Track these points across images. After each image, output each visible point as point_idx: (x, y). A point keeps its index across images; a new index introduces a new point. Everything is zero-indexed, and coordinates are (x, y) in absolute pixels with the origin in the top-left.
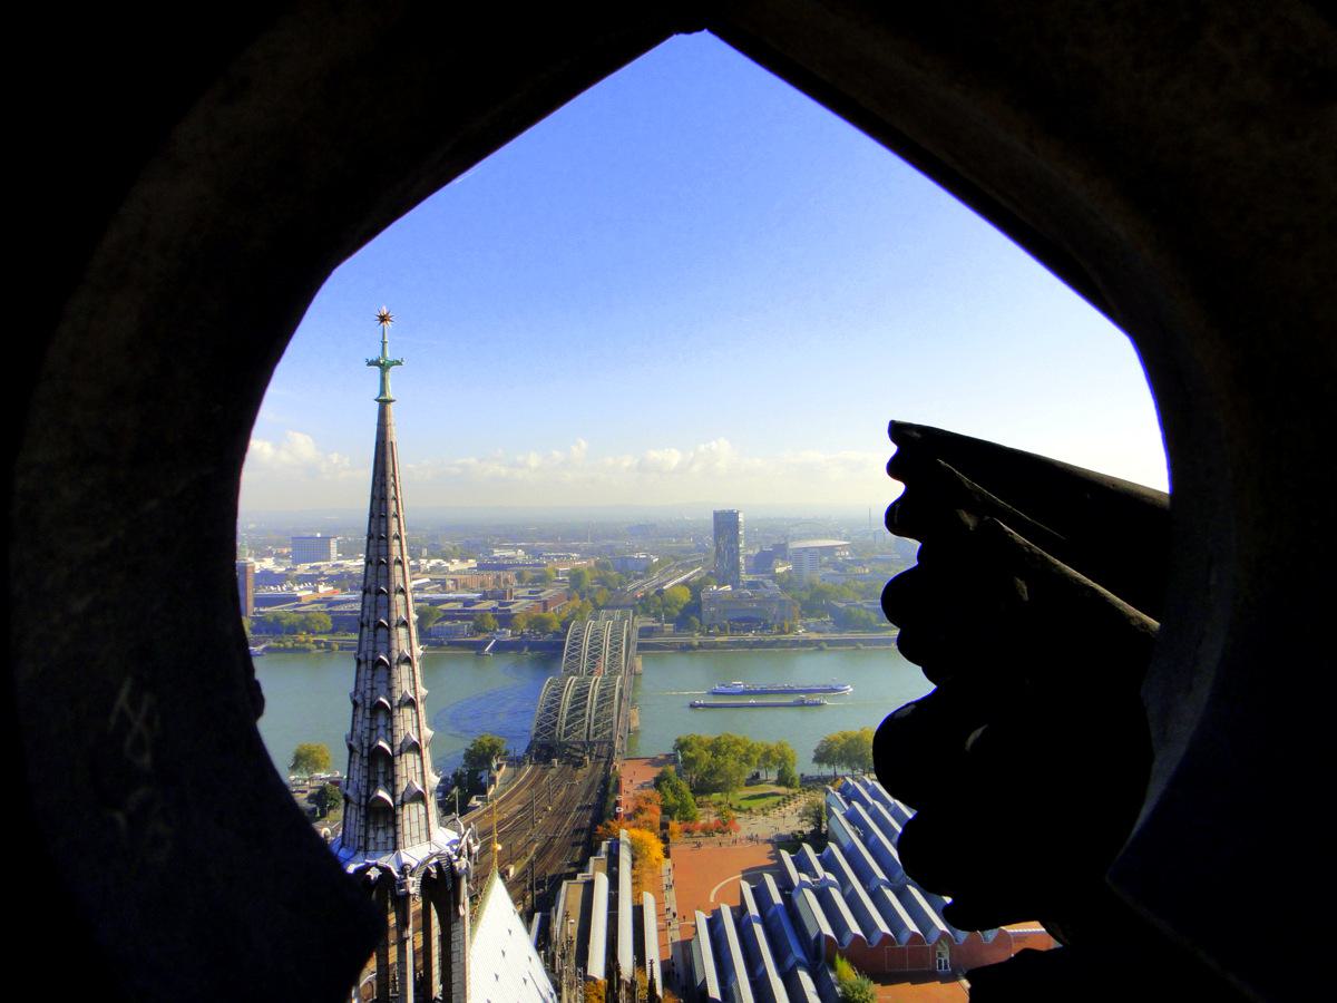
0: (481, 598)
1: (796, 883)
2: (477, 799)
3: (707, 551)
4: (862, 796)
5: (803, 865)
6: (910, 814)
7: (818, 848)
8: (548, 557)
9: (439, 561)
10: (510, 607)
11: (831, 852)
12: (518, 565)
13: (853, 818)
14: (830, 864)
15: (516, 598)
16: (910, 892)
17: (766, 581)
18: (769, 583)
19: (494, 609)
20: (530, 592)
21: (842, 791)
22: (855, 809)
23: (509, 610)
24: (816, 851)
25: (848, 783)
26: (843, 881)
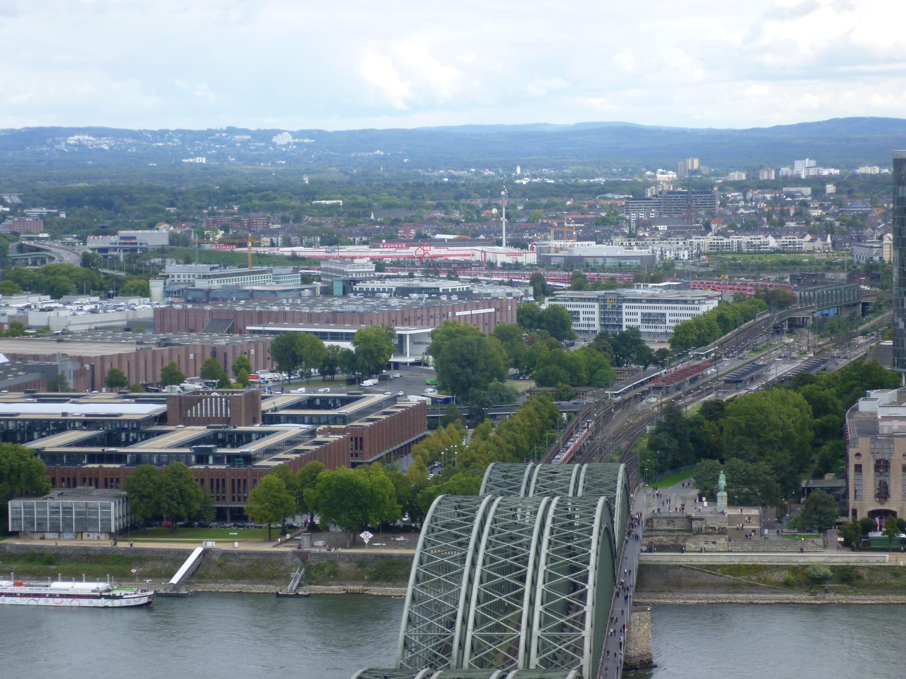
0: (162, 419)
23: (248, 459)
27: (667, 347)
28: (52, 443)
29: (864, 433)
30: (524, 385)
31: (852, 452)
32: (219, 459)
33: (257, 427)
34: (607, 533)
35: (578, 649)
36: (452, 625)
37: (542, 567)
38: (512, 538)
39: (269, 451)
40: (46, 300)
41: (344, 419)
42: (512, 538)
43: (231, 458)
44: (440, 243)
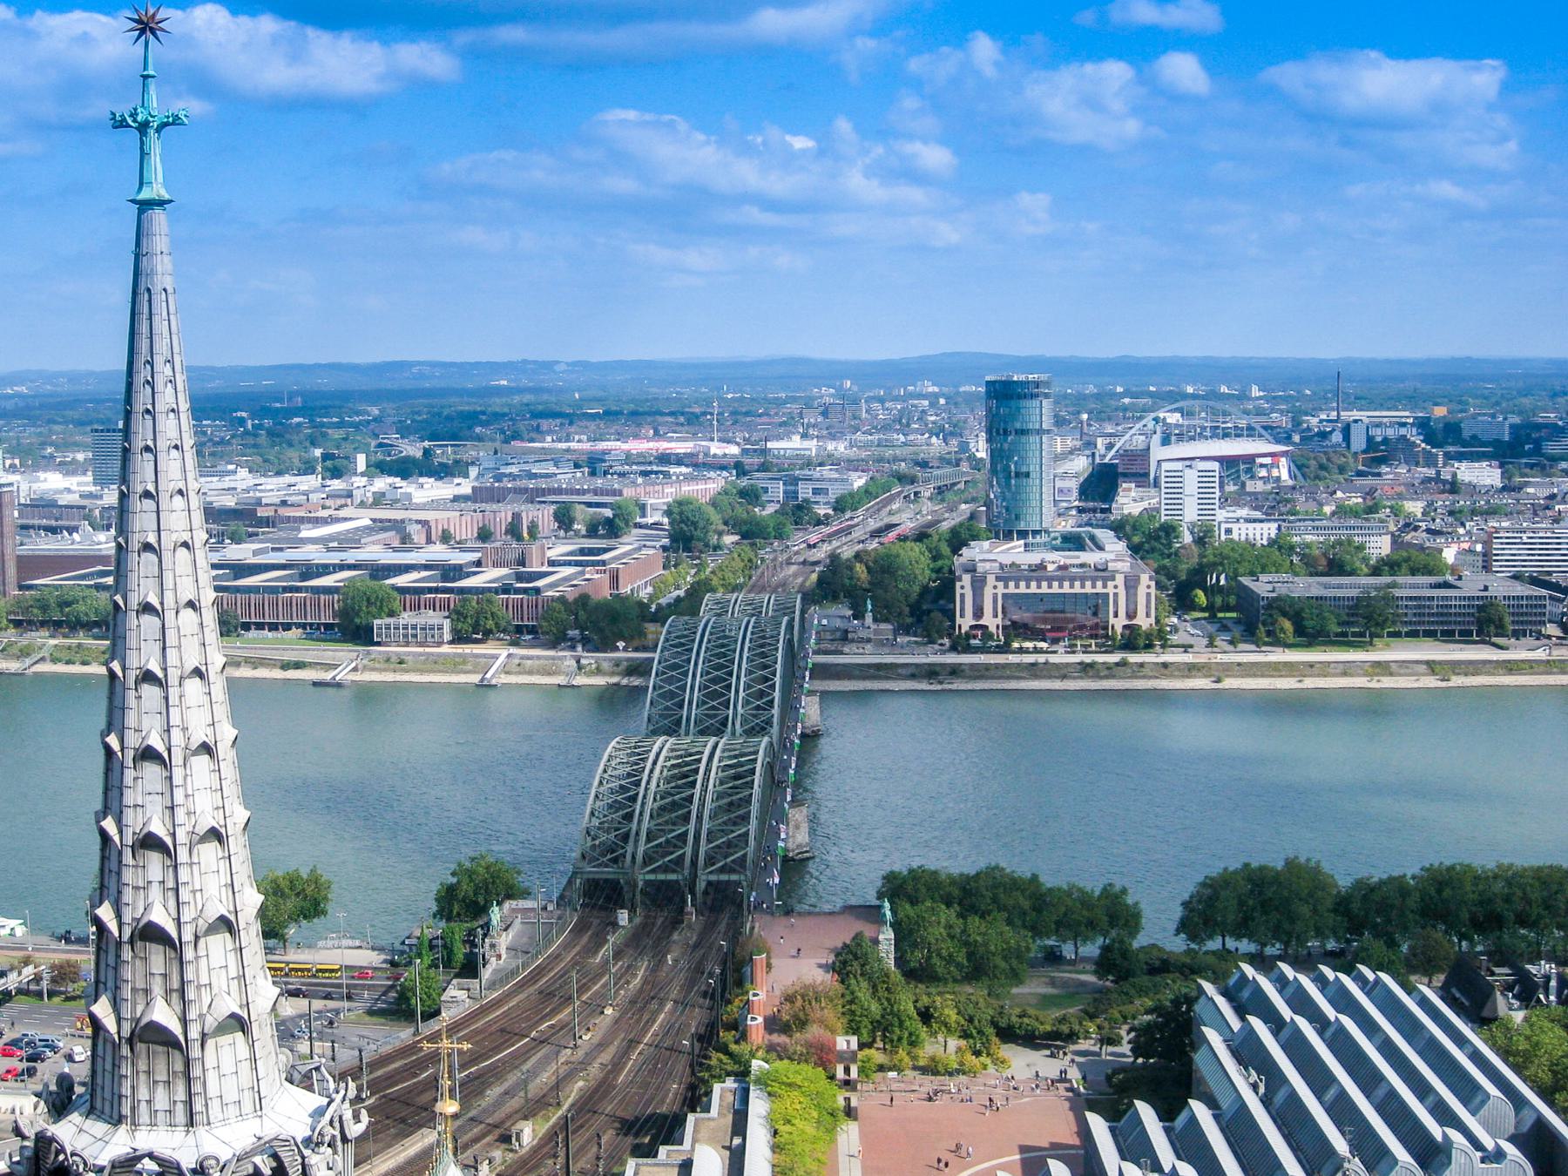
0: (478, 563)
3: (977, 464)
7: (1167, 1114)
8: (622, 475)
9: (390, 480)
10: (540, 583)
11: (1193, 1120)
12: (559, 491)
15: (552, 563)
17: (1099, 533)
18: (1104, 535)
19: (506, 589)
20: (582, 552)
22: (1252, 1031)
23: (537, 591)
25: (1243, 976)
27: (831, 512)
28: (402, 580)
29: (967, 571)
30: (729, 539)
31: (958, 584)
32: (517, 591)
33: (545, 569)
34: (790, 643)
35: (769, 722)
36: (681, 706)
37: (744, 666)
38: (723, 646)
39: (551, 586)
40: (397, 481)
41: (604, 563)
42: (723, 646)
43: (525, 591)
44: (671, 440)
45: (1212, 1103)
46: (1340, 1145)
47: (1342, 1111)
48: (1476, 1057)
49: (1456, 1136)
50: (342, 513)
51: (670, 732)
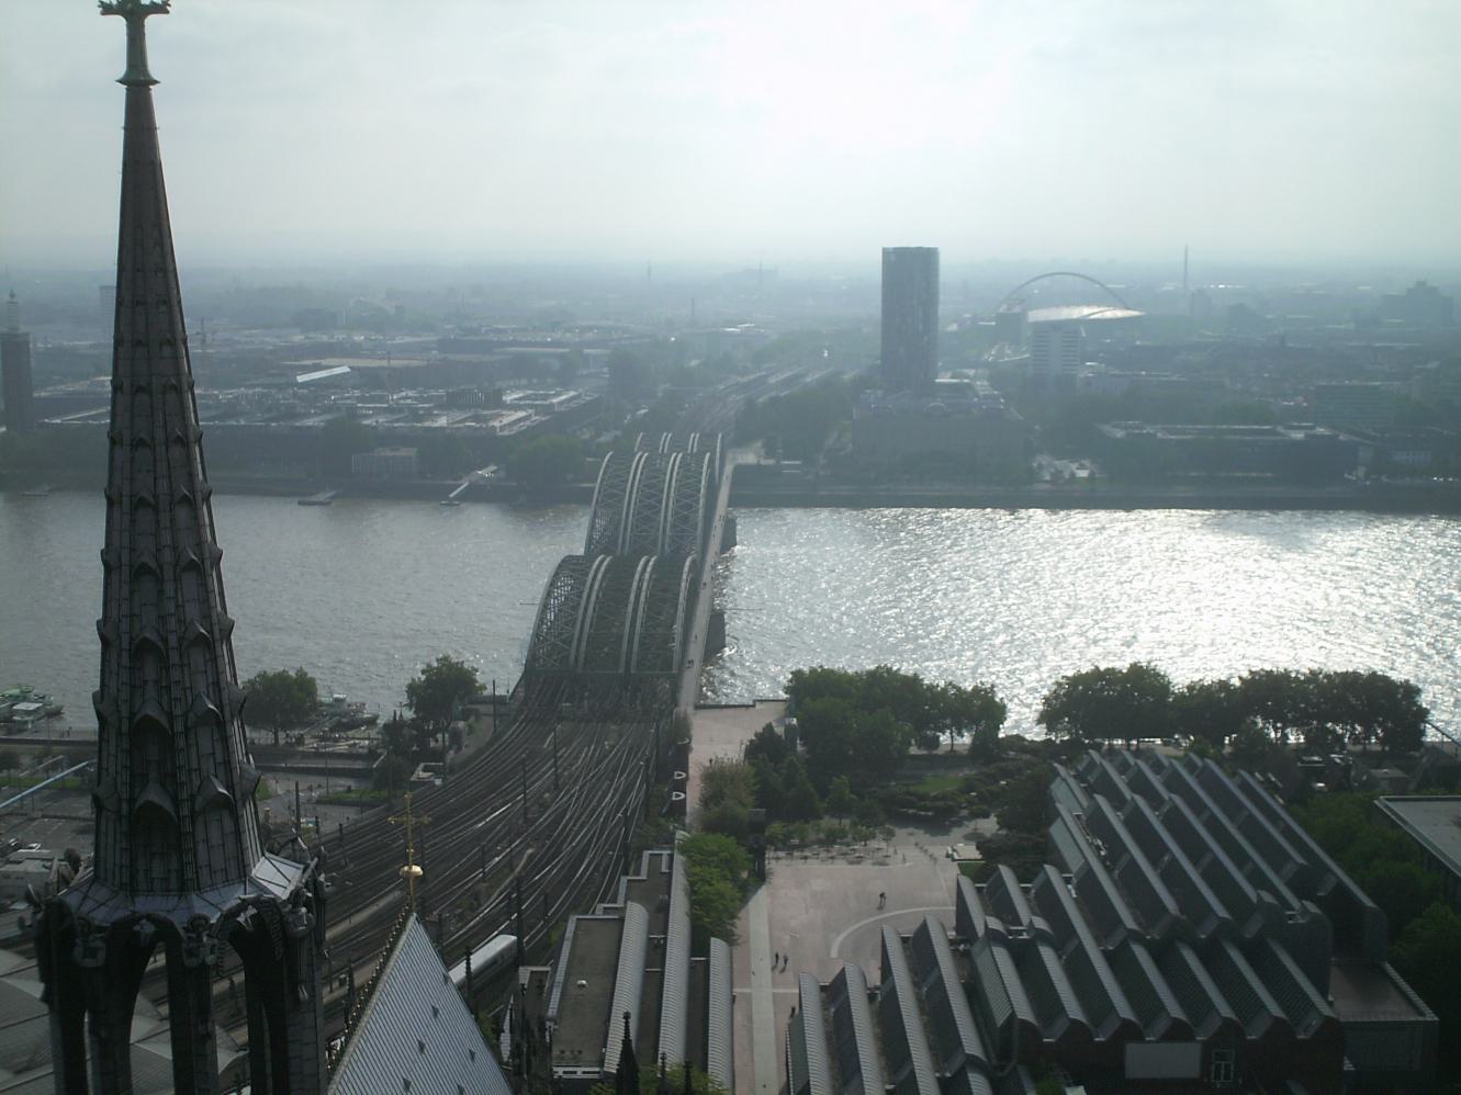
1: (980, 931)
2: (425, 770)
4: (1187, 785)
5: (998, 902)
6: (1376, 802)
11: (1048, 883)
12: (515, 343)
13: (1095, 824)
14: (1046, 902)
16: (1229, 958)
21: (1080, 777)
22: (1099, 807)
24: (1021, 879)
26: (1062, 936)
45: (1062, 867)
46: (1170, 903)
47: (1173, 876)
48: (1287, 832)
49: (1268, 898)
50: (324, 362)
51: (606, 551)
